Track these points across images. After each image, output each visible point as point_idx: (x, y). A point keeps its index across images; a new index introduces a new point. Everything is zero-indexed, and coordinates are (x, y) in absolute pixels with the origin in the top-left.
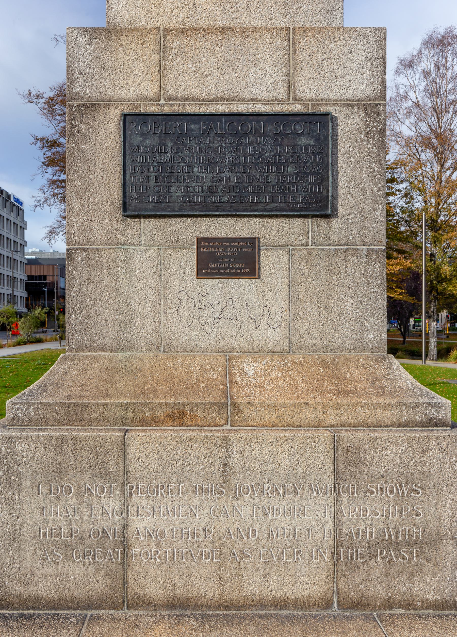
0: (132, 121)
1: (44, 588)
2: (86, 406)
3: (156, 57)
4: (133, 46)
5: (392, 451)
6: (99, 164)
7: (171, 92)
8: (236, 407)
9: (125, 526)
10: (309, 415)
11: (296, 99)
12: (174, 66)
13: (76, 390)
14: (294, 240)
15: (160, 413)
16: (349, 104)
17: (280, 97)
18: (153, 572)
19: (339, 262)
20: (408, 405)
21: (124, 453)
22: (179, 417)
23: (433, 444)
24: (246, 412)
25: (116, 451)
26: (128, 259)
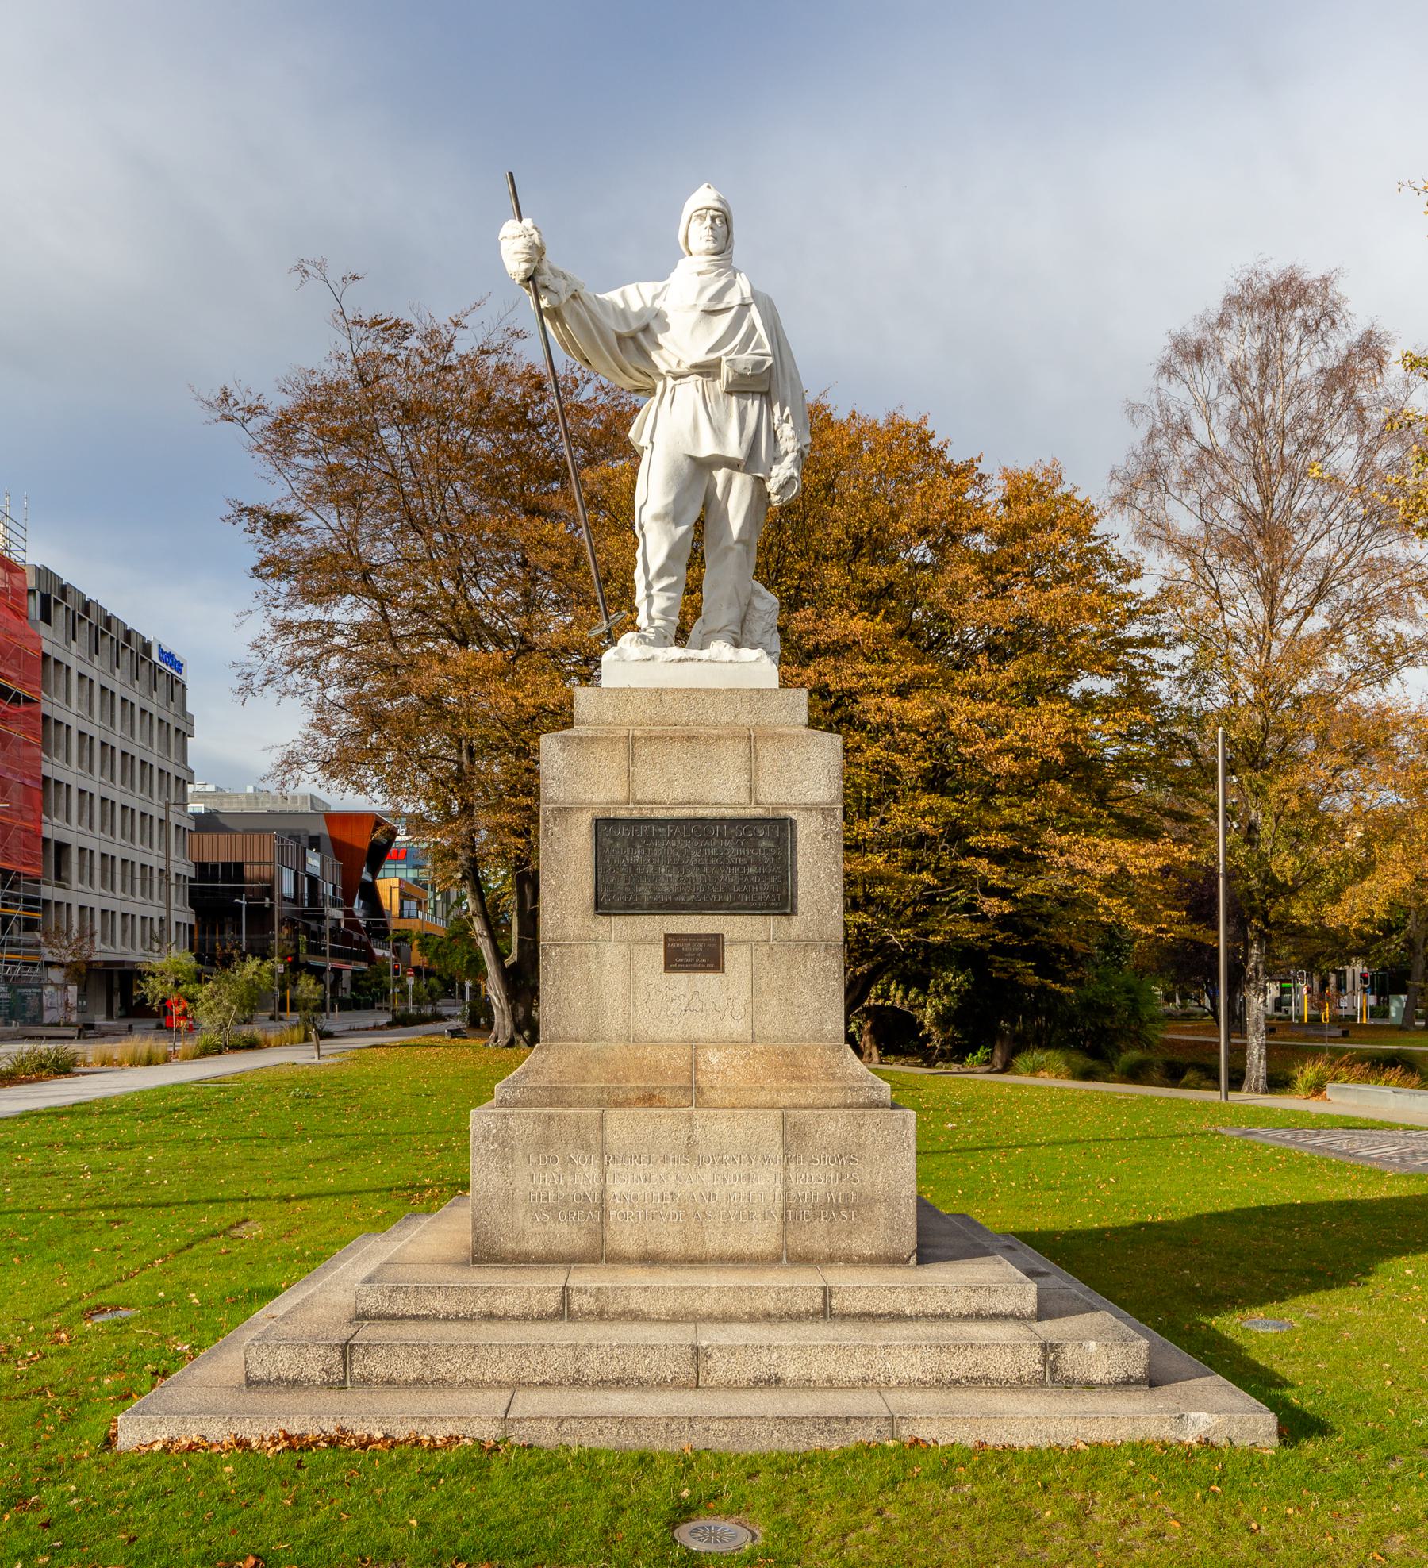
0: (604, 826)
1: (534, 1245)
2: (566, 1089)
3: (625, 764)
4: (604, 753)
5: (833, 1127)
7: (639, 797)
8: (700, 1090)
9: (604, 1191)
10: (765, 1097)
12: (642, 771)
13: (555, 1076)
15: (632, 1095)
16: (808, 808)
18: (627, 1231)
20: (852, 1089)
21: (602, 1127)
22: (649, 1099)
23: (868, 1120)
24: (708, 1095)
25: (595, 1126)
26: (599, 954)
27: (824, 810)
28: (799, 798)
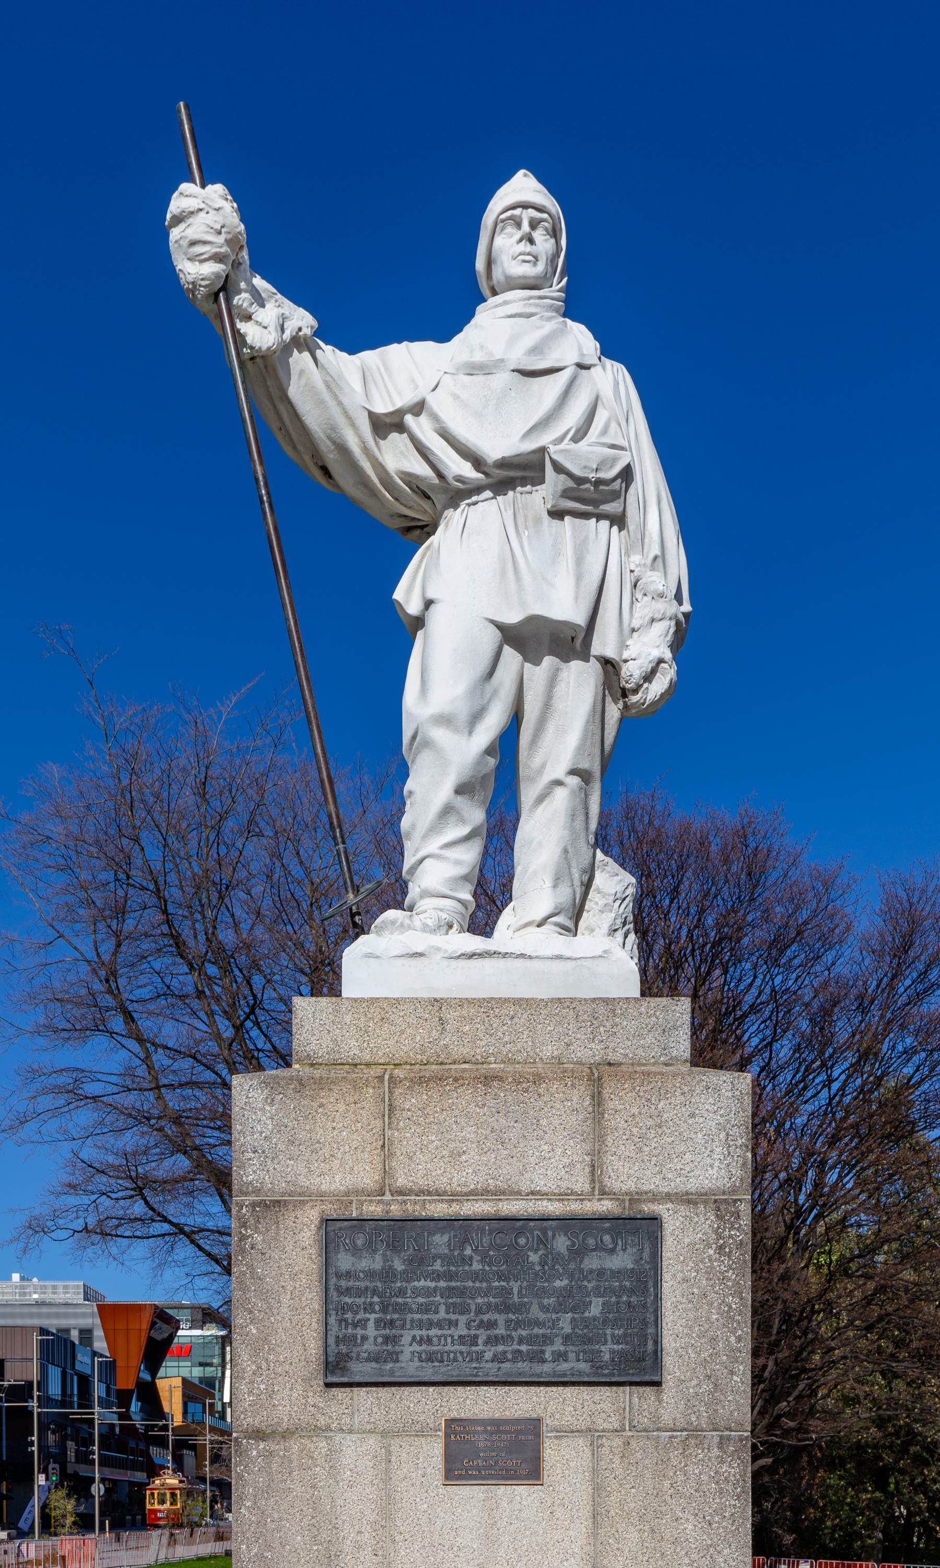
4: (341, 1107)
6: (286, 1299)
7: (401, 1182)
11: (603, 1193)
12: (406, 1138)
14: (601, 1424)
16: (689, 1199)
17: (578, 1188)
19: (675, 1457)
26: (333, 1454)
27: (719, 1203)
28: (678, 1184)
